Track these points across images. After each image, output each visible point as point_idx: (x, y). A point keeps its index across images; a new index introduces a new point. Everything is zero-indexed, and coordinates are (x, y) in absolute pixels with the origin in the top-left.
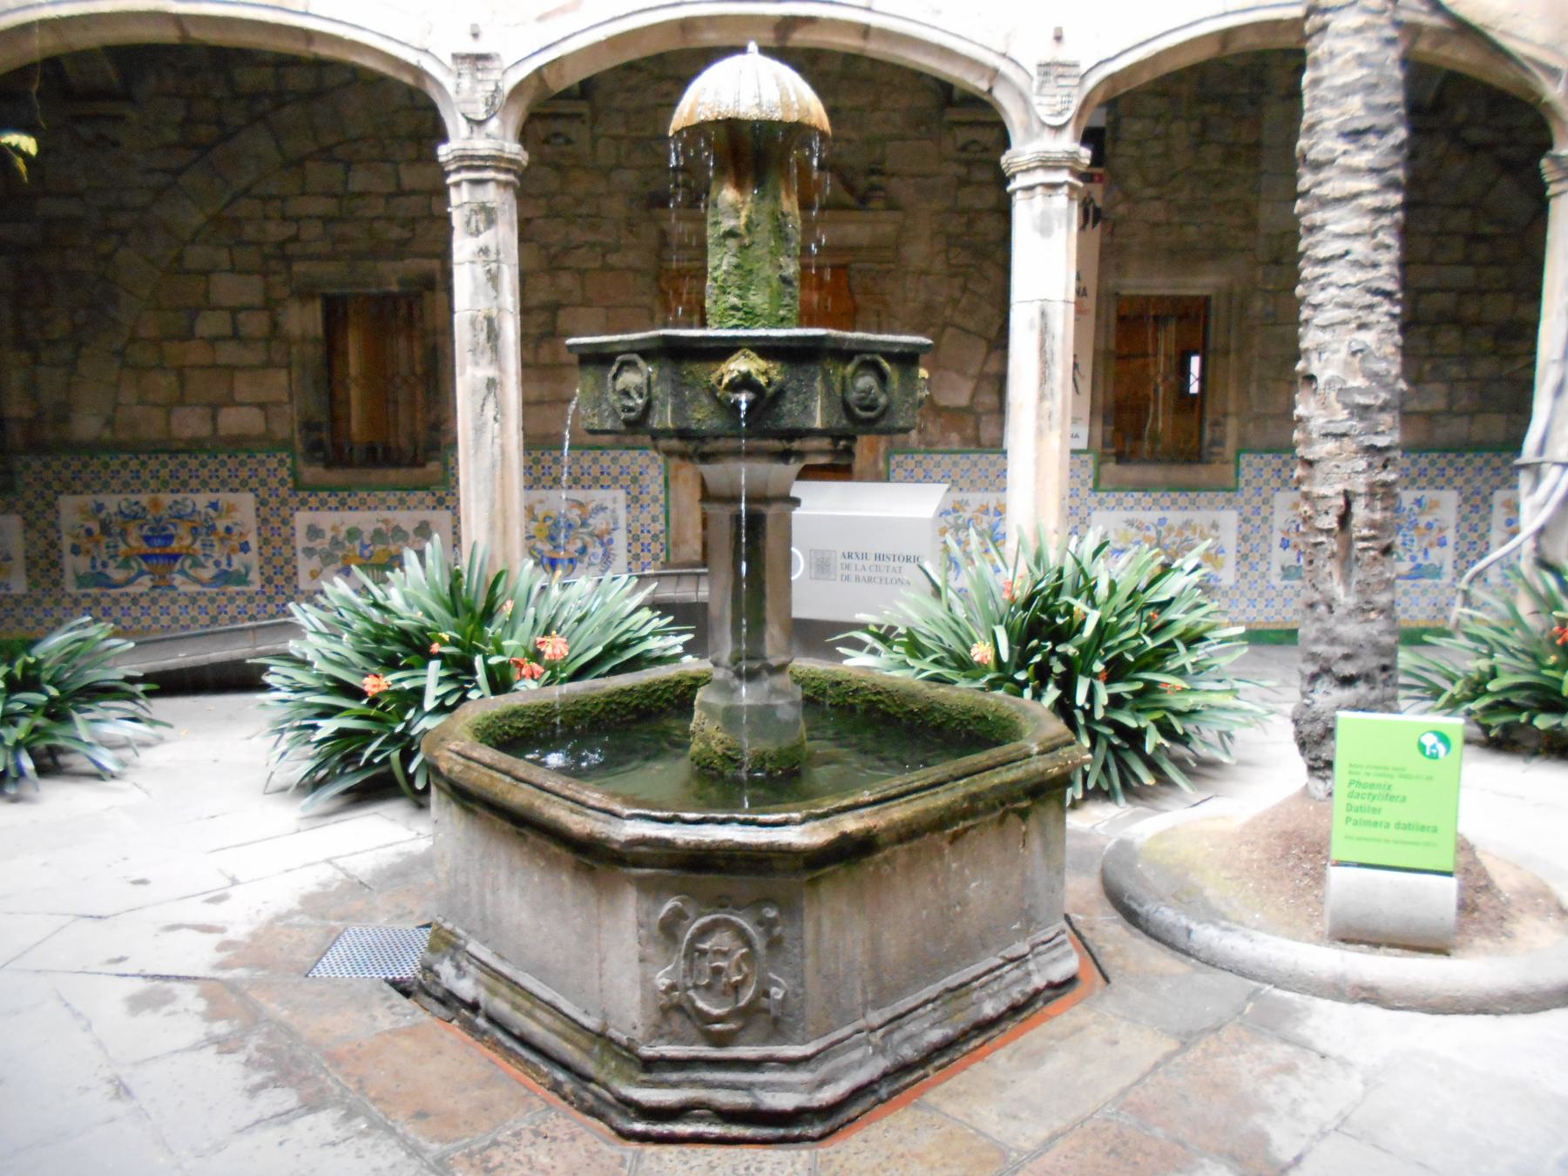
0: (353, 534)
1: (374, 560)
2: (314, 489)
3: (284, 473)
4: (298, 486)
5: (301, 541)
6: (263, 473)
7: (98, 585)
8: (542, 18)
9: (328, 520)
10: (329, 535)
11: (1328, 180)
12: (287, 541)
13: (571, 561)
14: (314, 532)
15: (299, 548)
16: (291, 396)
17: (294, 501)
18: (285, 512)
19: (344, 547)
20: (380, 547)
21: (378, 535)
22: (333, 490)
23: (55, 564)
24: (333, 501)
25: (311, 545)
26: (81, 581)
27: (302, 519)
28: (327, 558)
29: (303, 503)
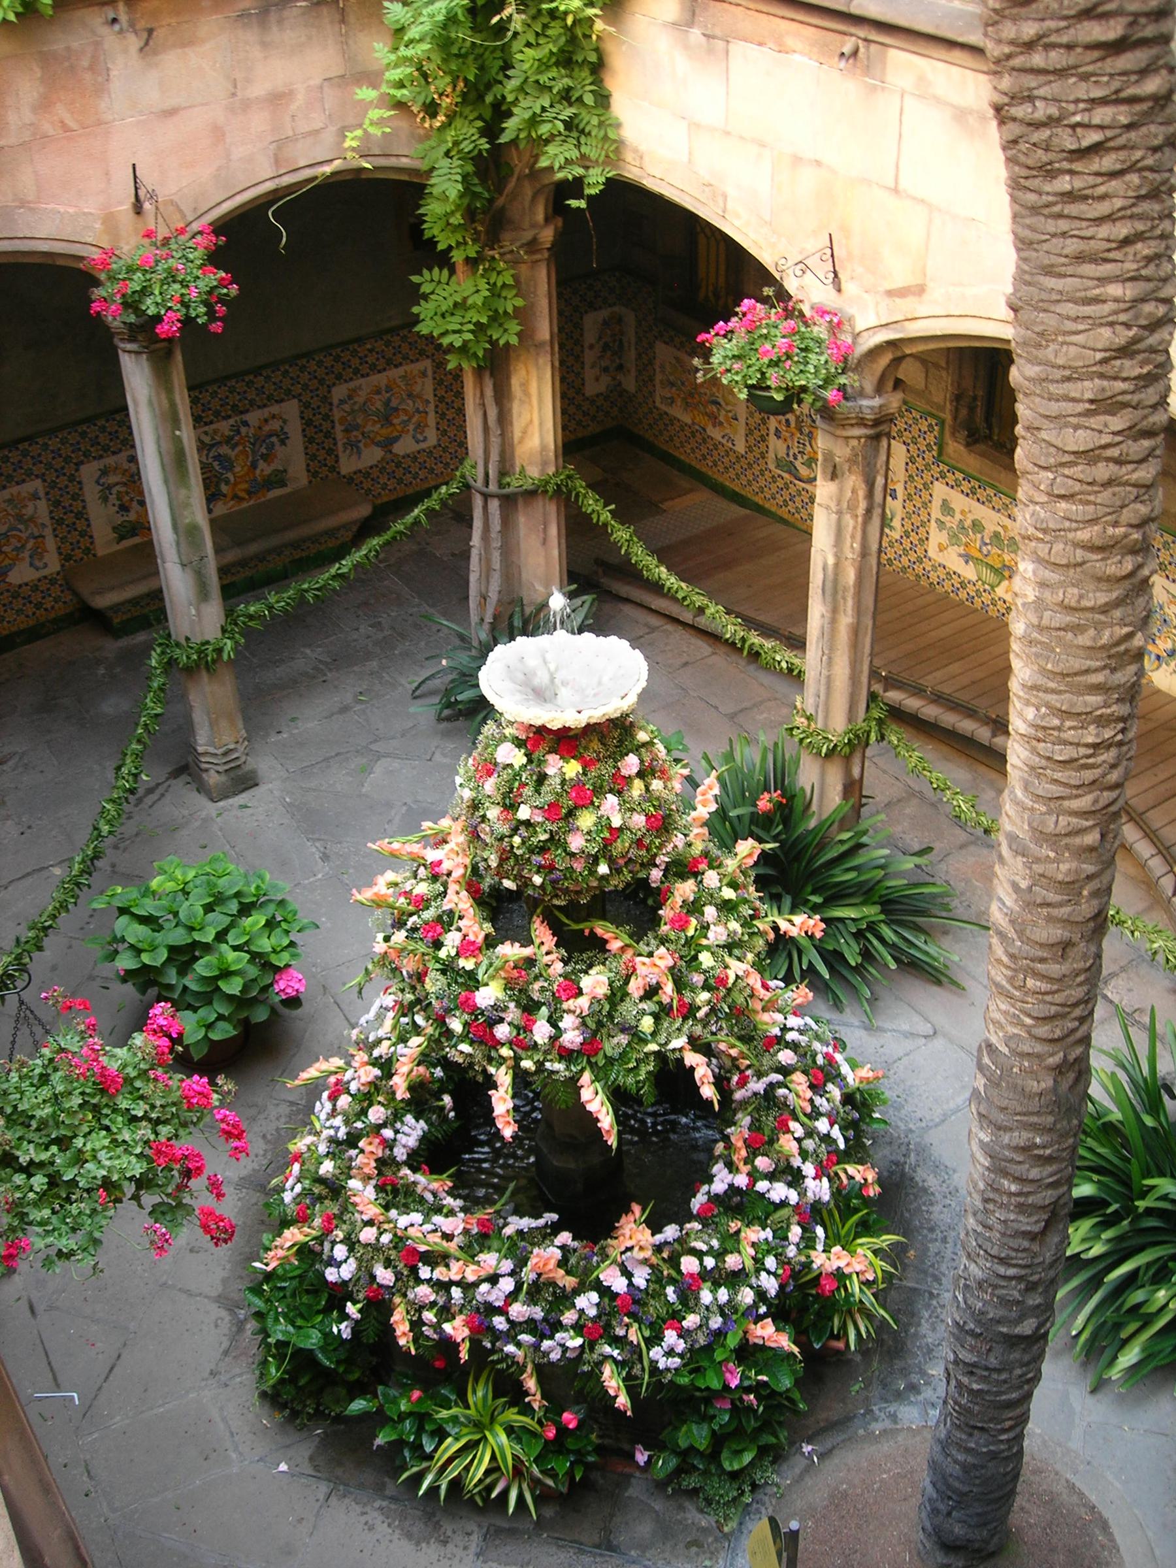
0: (977, 526)
1: (989, 560)
2: (953, 469)
3: (931, 439)
4: (939, 458)
5: (936, 512)
6: (915, 429)
7: (790, 473)
8: (890, 293)
9: (959, 501)
10: (958, 516)
11: (1051, 1175)
12: (925, 505)
13: (1158, 657)
14: (946, 508)
15: (933, 516)
16: (947, 363)
17: (935, 470)
18: (927, 476)
19: (967, 536)
20: (995, 551)
21: (996, 535)
22: (968, 477)
23: (763, 439)
24: (966, 486)
25: (943, 519)
26: (779, 463)
27: (940, 490)
28: (954, 539)
29: (943, 476)
